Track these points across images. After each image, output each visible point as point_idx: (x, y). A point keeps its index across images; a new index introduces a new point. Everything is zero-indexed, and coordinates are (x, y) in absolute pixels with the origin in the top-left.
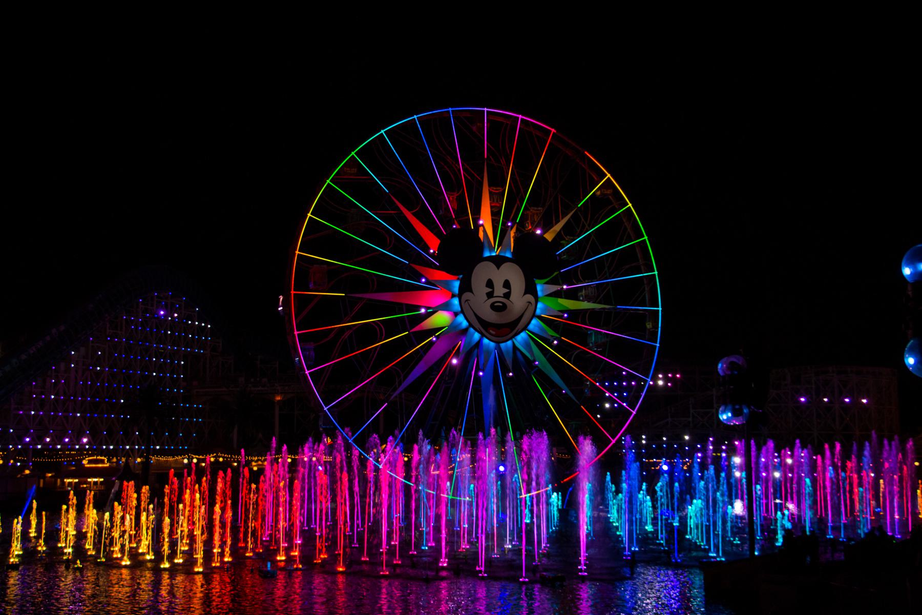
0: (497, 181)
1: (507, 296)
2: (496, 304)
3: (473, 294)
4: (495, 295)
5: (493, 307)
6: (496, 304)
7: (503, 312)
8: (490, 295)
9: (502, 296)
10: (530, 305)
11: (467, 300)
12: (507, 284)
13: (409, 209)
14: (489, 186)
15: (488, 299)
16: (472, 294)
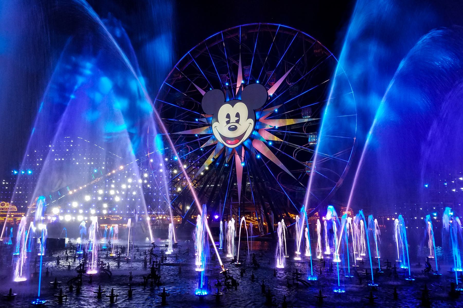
0: (246, 63)
1: (237, 121)
2: (231, 127)
3: (219, 123)
4: (230, 122)
5: (230, 129)
6: (231, 127)
7: (235, 131)
8: (228, 122)
9: (235, 122)
10: (251, 124)
11: (215, 127)
12: (238, 115)
13: (201, 87)
14: (242, 66)
15: (227, 124)
16: (217, 122)
